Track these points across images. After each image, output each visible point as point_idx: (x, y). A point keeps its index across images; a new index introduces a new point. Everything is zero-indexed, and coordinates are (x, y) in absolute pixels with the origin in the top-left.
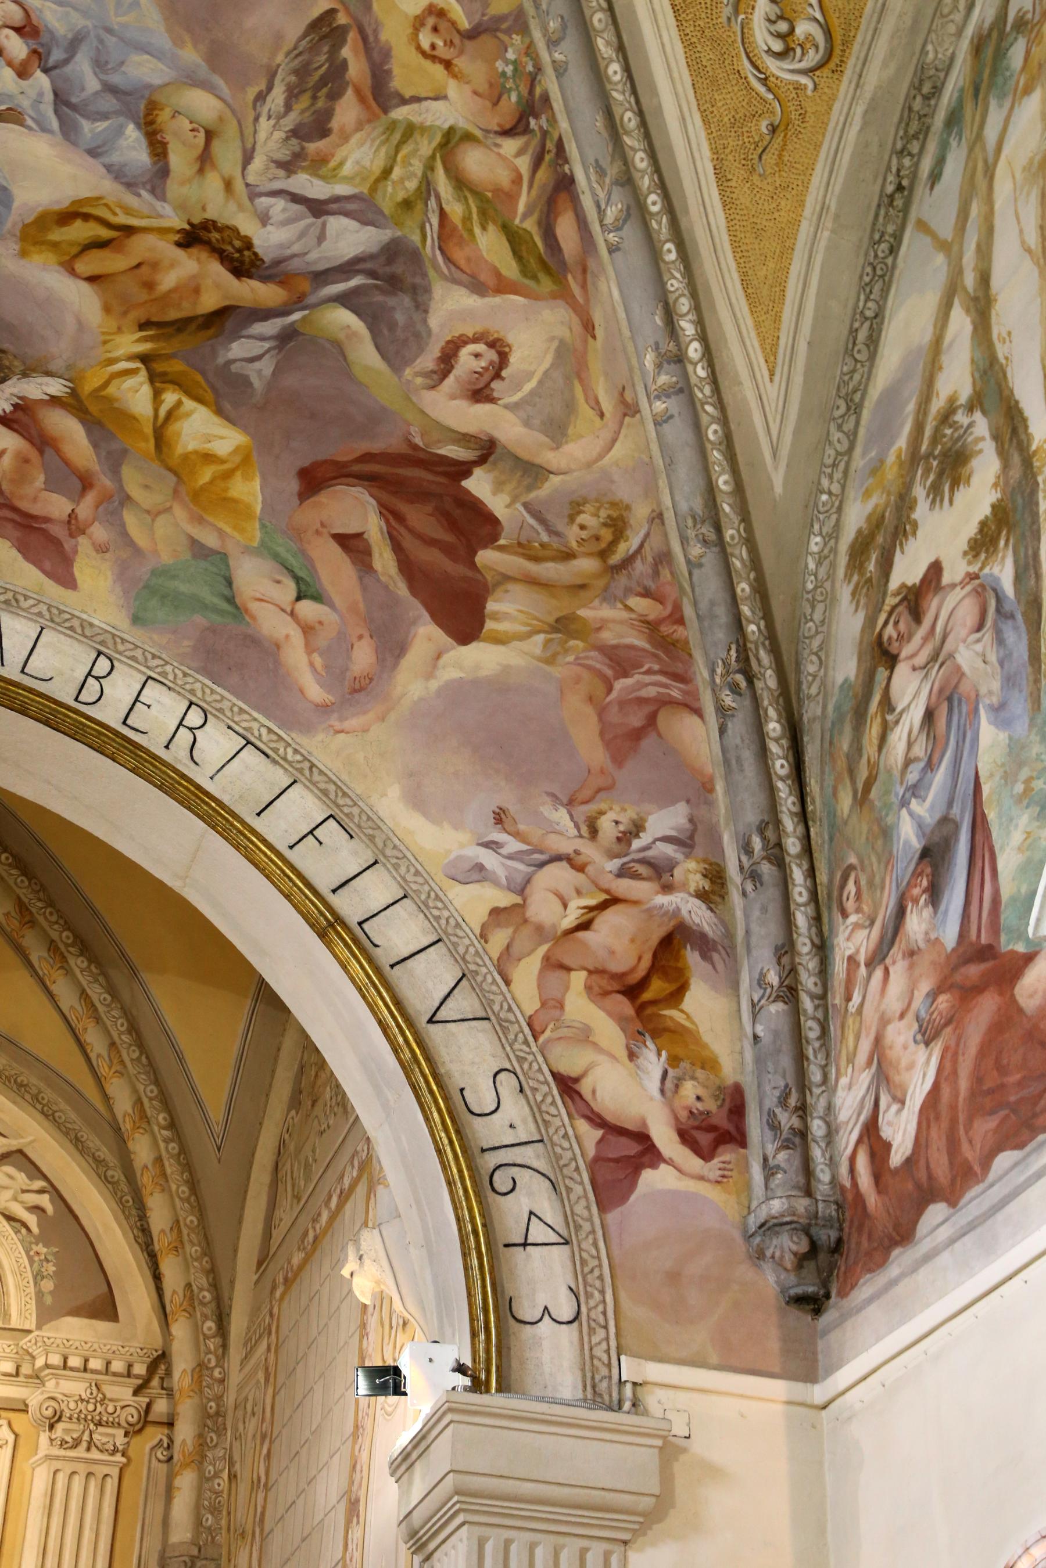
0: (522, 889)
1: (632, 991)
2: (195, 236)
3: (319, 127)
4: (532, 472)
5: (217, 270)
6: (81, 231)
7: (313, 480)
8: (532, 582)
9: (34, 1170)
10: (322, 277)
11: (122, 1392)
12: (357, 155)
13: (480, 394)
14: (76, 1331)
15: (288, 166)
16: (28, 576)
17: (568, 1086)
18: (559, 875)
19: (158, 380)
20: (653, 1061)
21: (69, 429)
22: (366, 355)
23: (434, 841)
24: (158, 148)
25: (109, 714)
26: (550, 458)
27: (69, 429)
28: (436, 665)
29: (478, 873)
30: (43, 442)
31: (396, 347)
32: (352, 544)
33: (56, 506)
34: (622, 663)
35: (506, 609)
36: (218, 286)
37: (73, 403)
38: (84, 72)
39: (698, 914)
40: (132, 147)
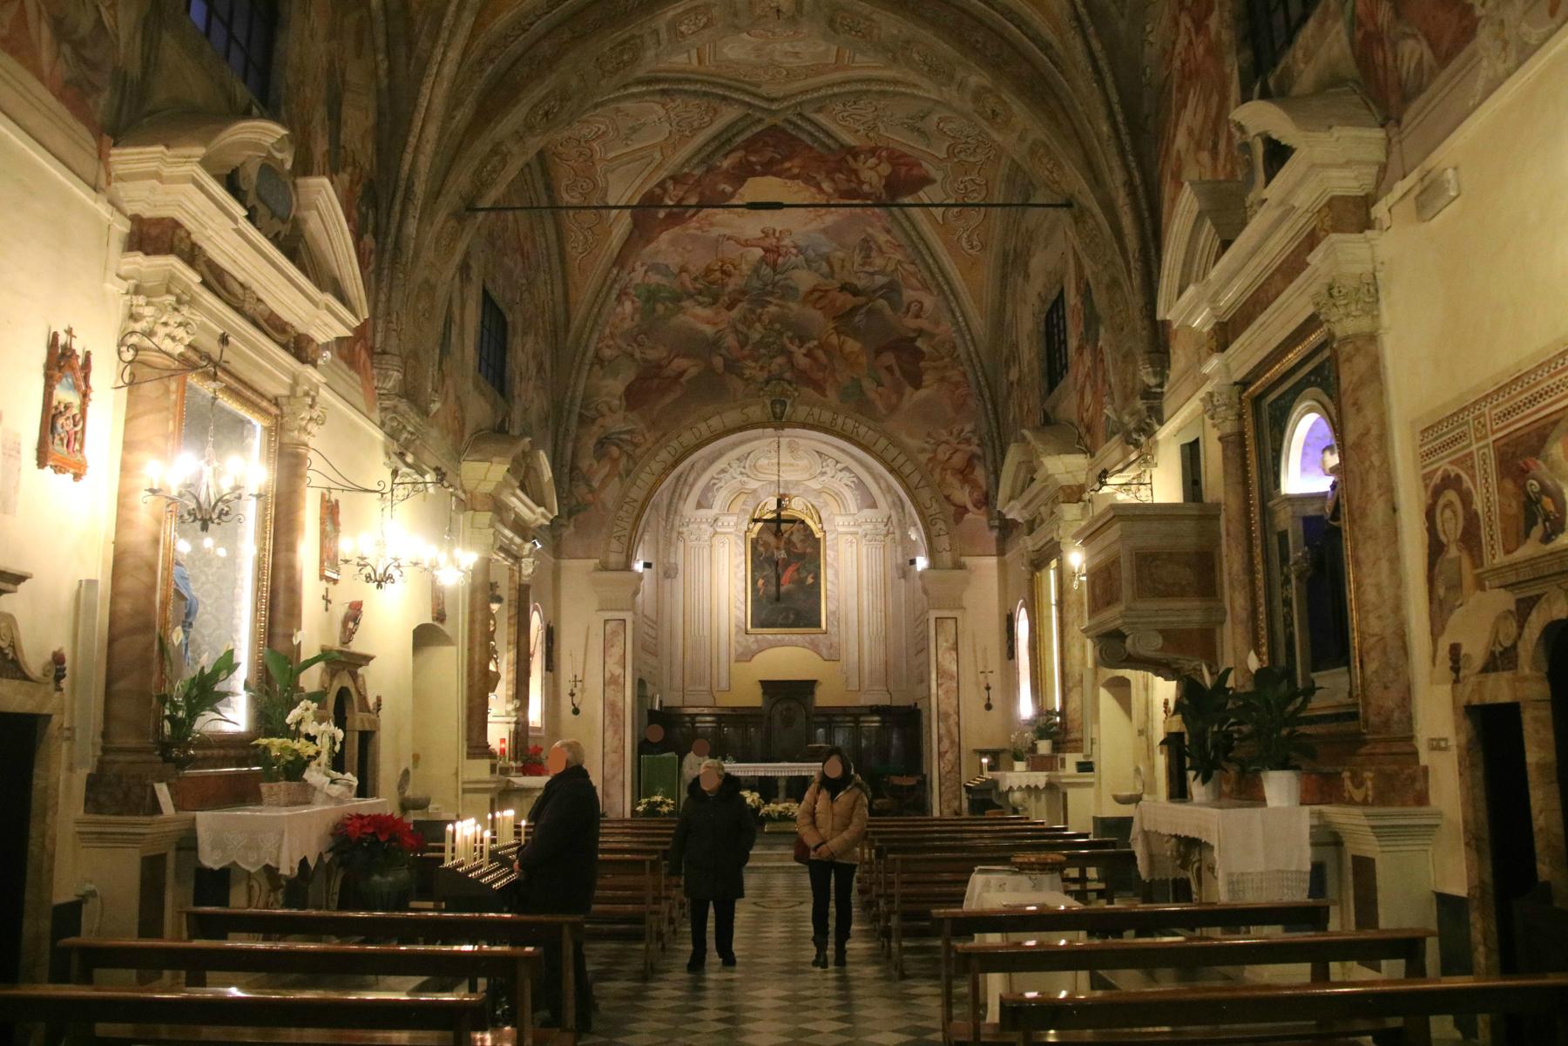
0: (935, 452)
1: (961, 472)
2: (844, 288)
3: (868, 256)
4: (932, 336)
5: (850, 297)
6: (817, 295)
7: (878, 353)
8: (935, 368)
9: (851, 471)
10: (874, 292)
11: (881, 526)
12: (879, 262)
13: (917, 316)
14: (868, 512)
15: (864, 264)
16: (816, 395)
17: (947, 498)
18: (943, 447)
19: (838, 333)
20: (967, 489)
21: (820, 354)
22: (888, 311)
23: (913, 443)
24: (831, 266)
25: (838, 428)
26: (937, 331)
27: (820, 354)
28: (913, 397)
29: (923, 450)
30: (815, 359)
31: (895, 306)
32: (889, 369)
33: (820, 375)
34: (957, 385)
35: (928, 378)
36: (847, 300)
37: (821, 346)
38: (811, 253)
39: (978, 451)
40: (825, 268)
